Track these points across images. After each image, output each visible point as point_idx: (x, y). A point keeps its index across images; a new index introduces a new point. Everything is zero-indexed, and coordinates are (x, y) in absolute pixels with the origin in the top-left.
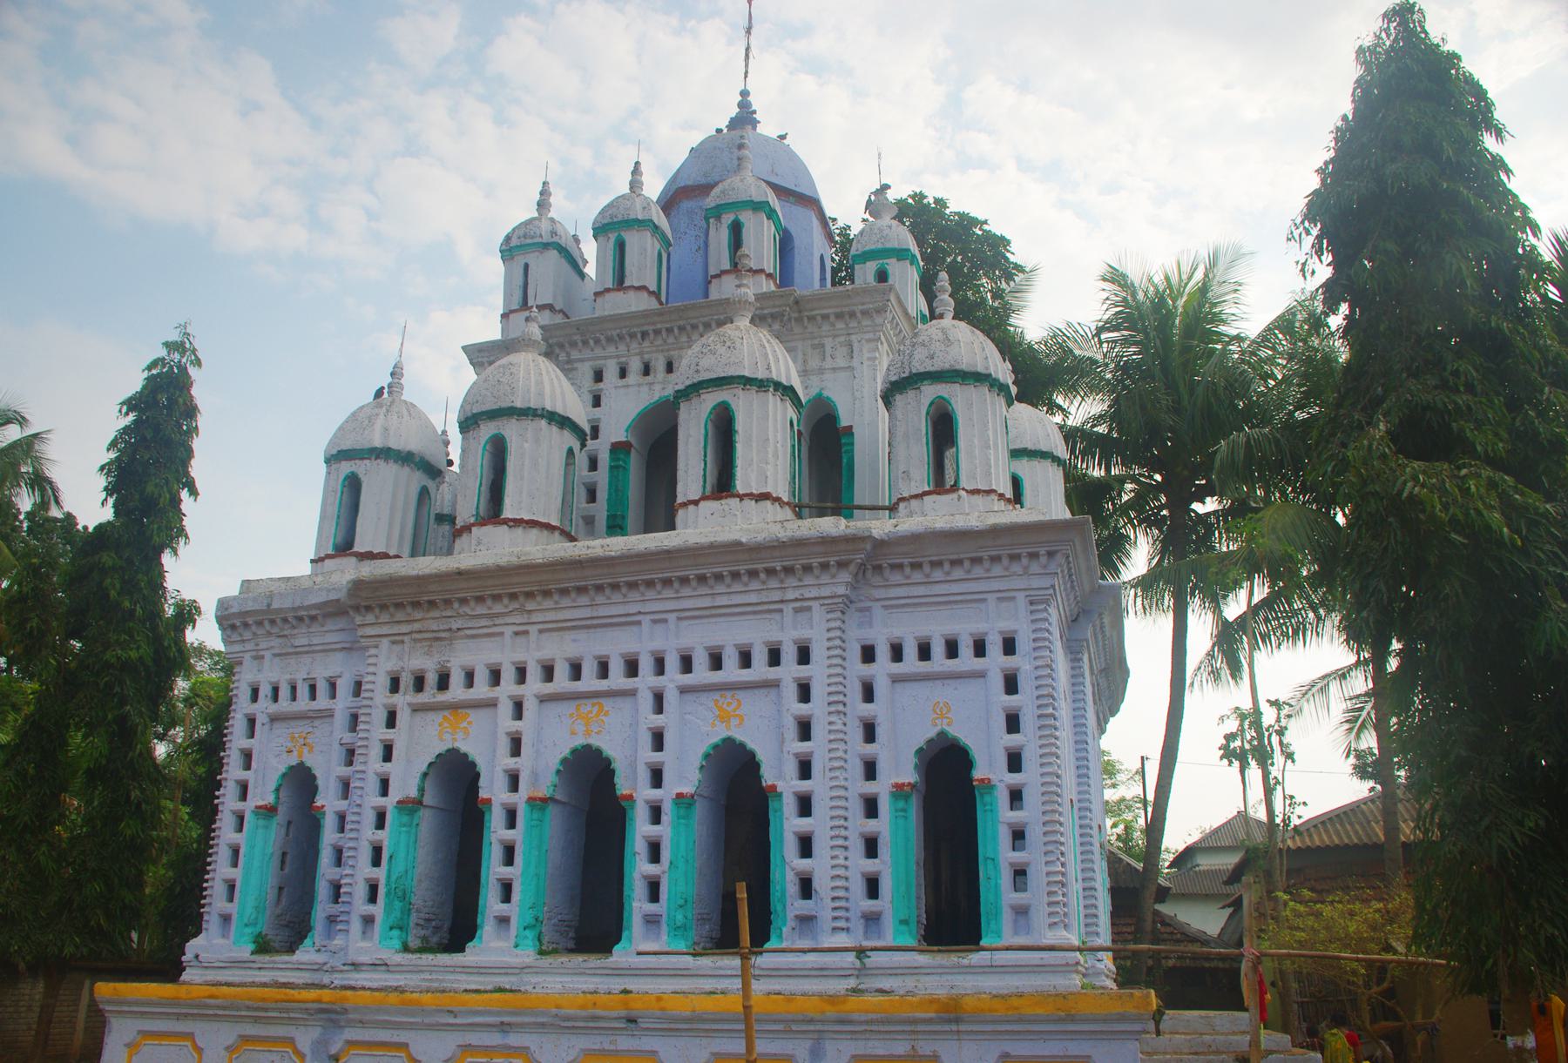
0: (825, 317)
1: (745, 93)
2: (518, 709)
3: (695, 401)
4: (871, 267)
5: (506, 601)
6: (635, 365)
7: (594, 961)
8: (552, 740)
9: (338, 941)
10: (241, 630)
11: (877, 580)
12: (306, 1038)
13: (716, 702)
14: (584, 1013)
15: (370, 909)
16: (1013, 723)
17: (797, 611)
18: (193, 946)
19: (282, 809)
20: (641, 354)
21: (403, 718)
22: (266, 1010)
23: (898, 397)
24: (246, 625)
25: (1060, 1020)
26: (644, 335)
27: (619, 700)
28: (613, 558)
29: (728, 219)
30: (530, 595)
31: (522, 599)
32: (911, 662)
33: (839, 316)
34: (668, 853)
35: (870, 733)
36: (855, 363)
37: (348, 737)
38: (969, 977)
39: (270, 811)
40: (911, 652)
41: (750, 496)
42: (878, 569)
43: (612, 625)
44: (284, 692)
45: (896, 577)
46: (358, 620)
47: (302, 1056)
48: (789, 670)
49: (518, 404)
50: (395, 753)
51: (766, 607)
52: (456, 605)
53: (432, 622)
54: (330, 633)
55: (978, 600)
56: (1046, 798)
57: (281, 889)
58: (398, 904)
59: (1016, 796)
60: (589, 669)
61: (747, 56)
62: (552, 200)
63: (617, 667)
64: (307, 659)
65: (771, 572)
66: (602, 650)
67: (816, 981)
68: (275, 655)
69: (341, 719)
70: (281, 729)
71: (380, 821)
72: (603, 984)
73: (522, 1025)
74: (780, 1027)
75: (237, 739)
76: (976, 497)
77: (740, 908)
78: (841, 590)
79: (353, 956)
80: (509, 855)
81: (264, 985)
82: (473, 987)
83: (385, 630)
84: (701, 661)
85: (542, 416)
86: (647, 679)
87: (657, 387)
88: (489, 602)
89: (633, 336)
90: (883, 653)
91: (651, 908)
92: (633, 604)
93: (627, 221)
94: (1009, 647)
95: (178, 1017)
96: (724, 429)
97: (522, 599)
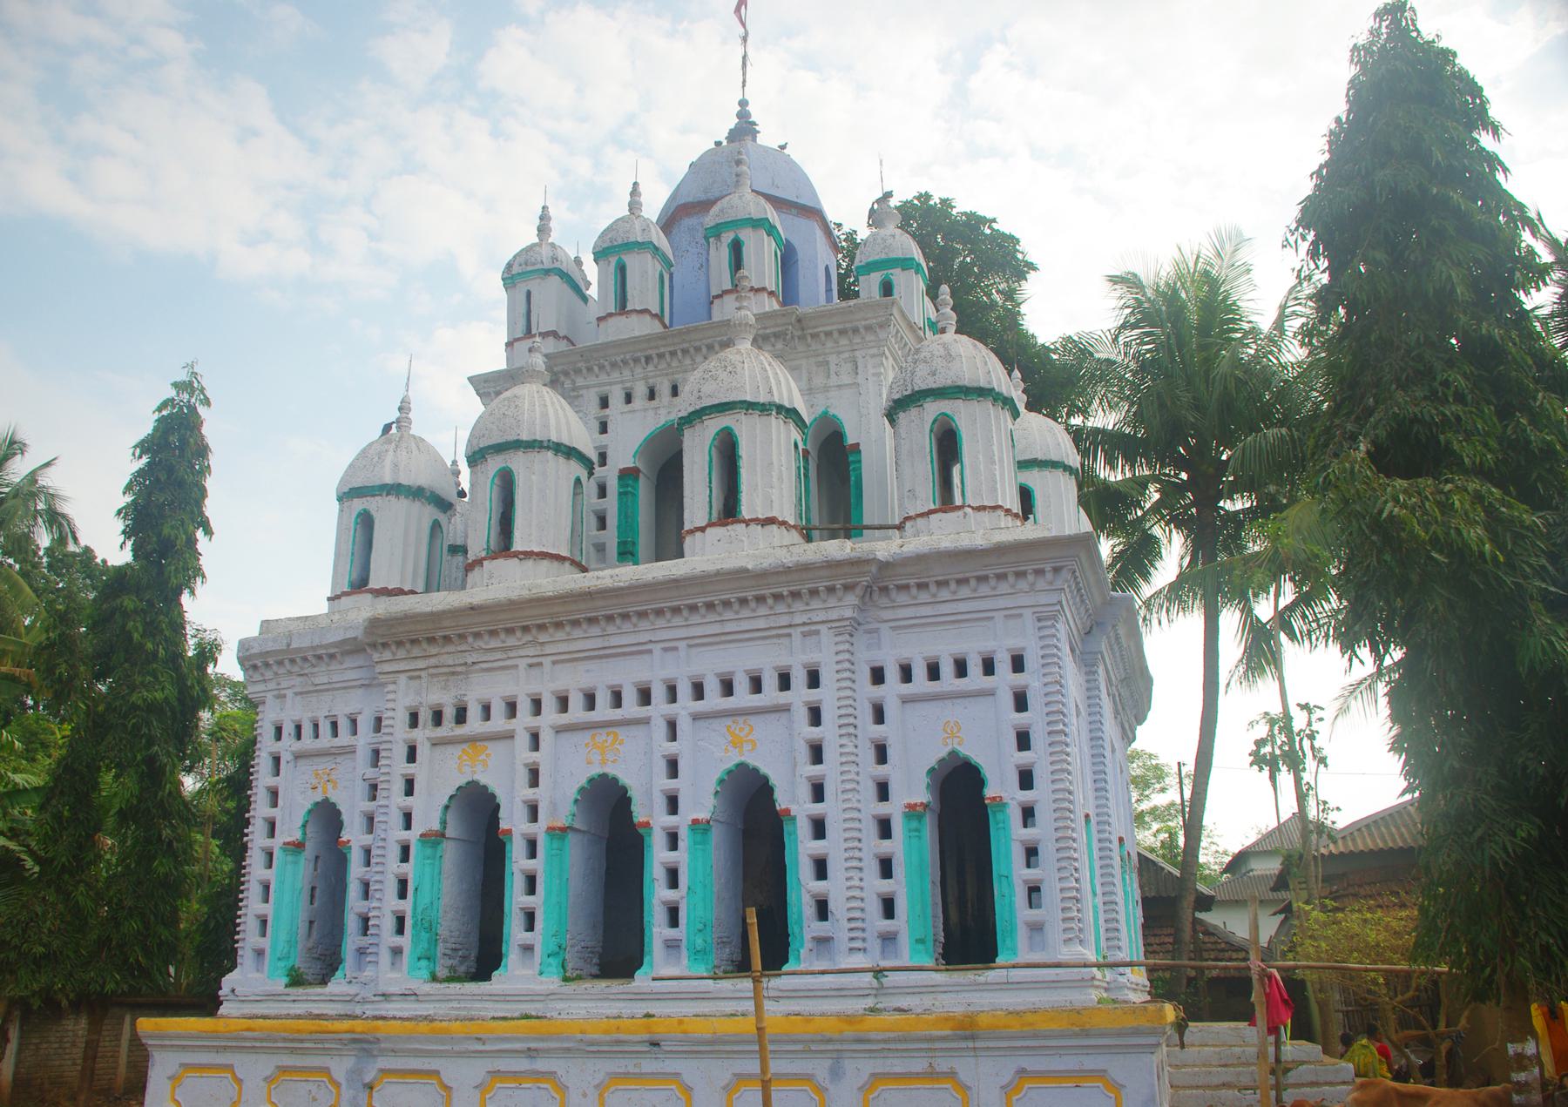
0: (828, 334)
1: (743, 103)
3: (698, 427)
4: (876, 278)
5: (519, 634)
6: (640, 390)
7: (616, 986)
8: (569, 769)
9: (369, 972)
10: (262, 670)
11: (884, 601)
12: (340, 1067)
14: (608, 1038)
15: (398, 940)
16: (1023, 741)
17: (805, 635)
18: (228, 981)
19: (308, 845)
20: (645, 378)
22: (302, 1041)
23: (901, 415)
24: (267, 665)
25: (1076, 1035)
26: (648, 359)
27: (633, 728)
28: (622, 589)
29: (728, 238)
30: (542, 627)
31: (534, 631)
33: (842, 332)
34: (687, 878)
35: (881, 754)
36: (860, 379)
37: (371, 773)
38: (985, 994)
39: (298, 846)
40: (920, 672)
41: (756, 520)
43: (624, 654)
44: (307, 730)
45: (902, 598)
46: (376, 656)
47: (337, 1085)
48: (800, 694)
49: (525, 437)
51: (774, 632)
52: (470, 639)
53: (448, 656)
54: (348, 671)
55: (985, 617)
57: (311, 922)
58: (425, 935)
59: (1028, 814)
60: (603, 699)
61: (744, 64)
63: (630, 696)
65: (778, 597)
66: (615, 680)
67: (834, 1001)
69: (363, 755)
71: (405, 855)
72: (626, 1008)
73: (548, 1051)
75: (262, 777)
76: (982, 513)
77: (762, 932)
78: (848, 613)
79: (382, 989)
80: (531, 884)
81: (299, 1017)
83: (402, 666)
84: (712, 687)
85: (548, 448)
86: (660, 707)
87: (663, 411)
88: (503, 636)
89: (636, 360)
90: (892, 674)
92: (643, 632)
94: (1018, 664)
95: (218, 1049)
96: (728, 452)
97: (534, 631)
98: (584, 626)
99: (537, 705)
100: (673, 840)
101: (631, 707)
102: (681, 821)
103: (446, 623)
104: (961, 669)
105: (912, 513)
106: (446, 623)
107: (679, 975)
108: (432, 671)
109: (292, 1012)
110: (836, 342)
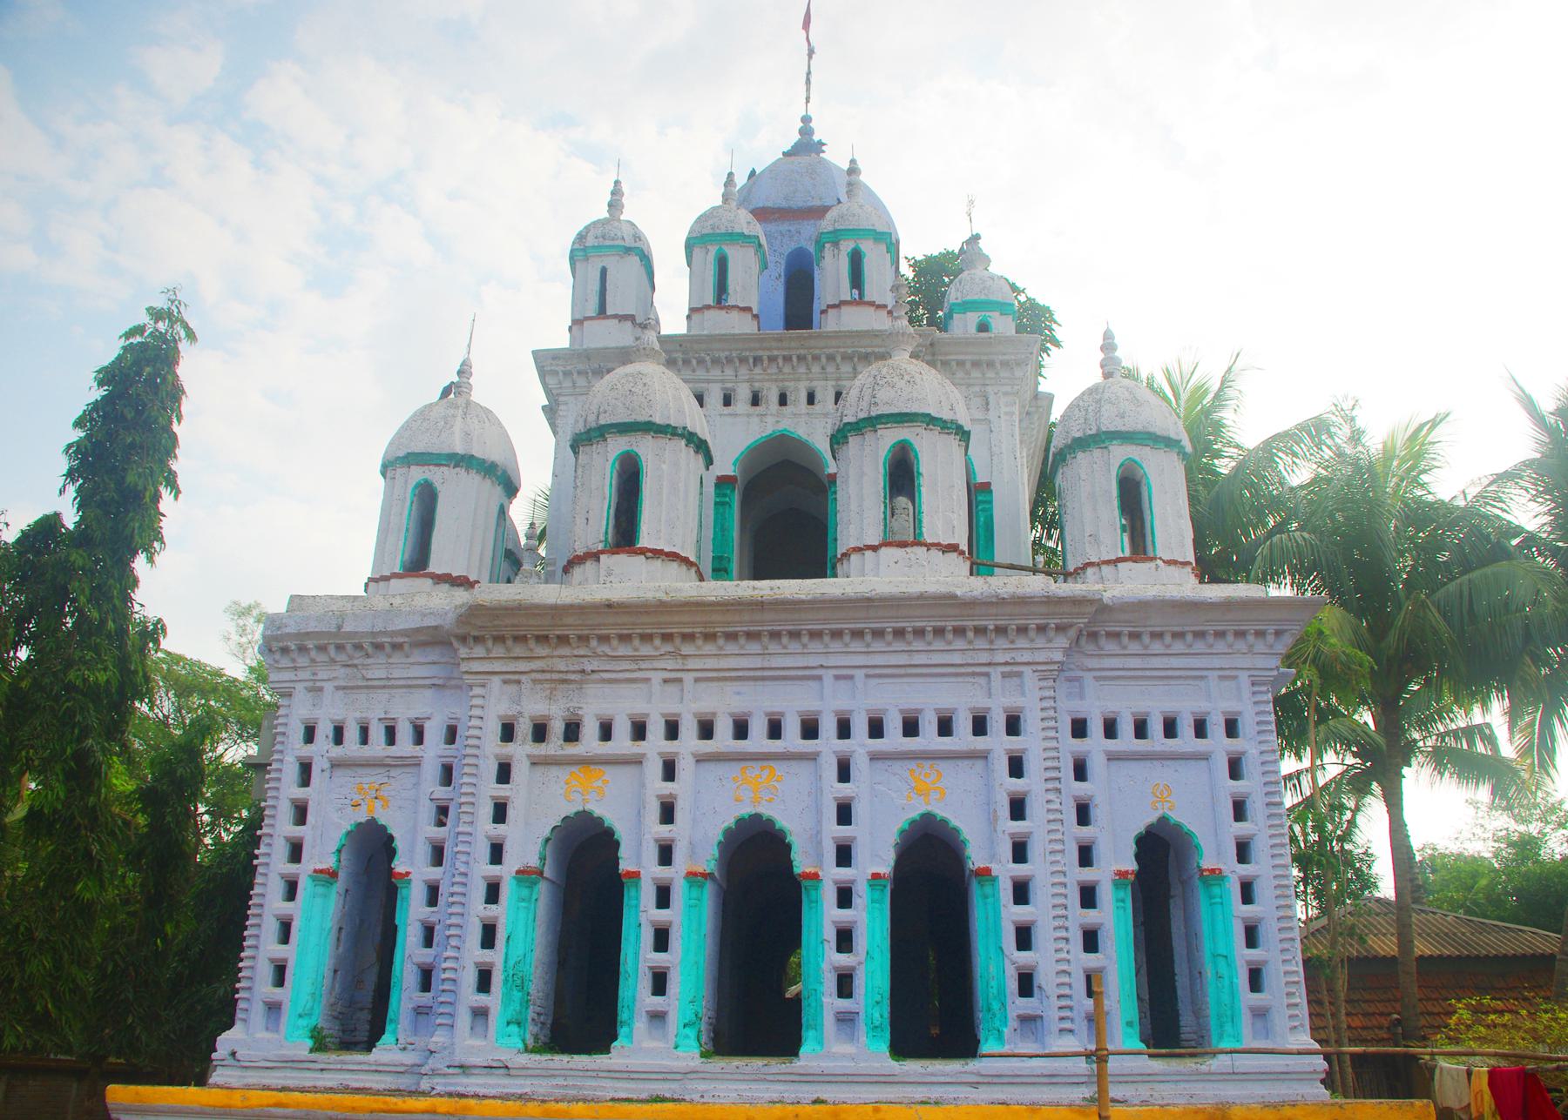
0: (961, 364)
1: (806, 120)
2: (669, 772)
3: (869, 436)
4: (973, 319)
5: (657, 642)
6: (743, 393)
7: (776, 1065)
8: (711, 809)
9: (439, 1038)
10: (295, 655)
11: (1089, 648)
15: (482, 999)
16: (1239, 811)
17: (1005, 675)
18: (227, 1041)
19: (342, 875)
21: (520, 771)
23: (1080, 455)
24: (302, 649)
26: (757, 360)
27: (793, 763)
28: (803, 602)
29: (847, 247)
30: (688, 637)
31: (678, 641)
32: (1126, 740)
33: (976, 364)
34: (848, 946)
35: (1083, 814)
36: (992, 415)
37: (442, 792)
38: (1208, 1085)
40: (1126, 728)
41: (937, 545)
42: (1093, 636)
44: (351, 734)
45: (1110, 646)
46: (463, 652)
48: (998, 742)
49: (658, 420)
50: (510, 813)
51: (970, 670)
52: (594, 643)
54: (418, 666)
56: (1278, 892)
58: (517, 995)
60: (758, 728)
61: (808, 81)
62: (624, 200)
63: (792, 728)
64: (383, 695)
65: (980, 631)
67: (1045, 1089)
68: (338, 688)
69: (431, 771)
70: (342, 776)
72: (790, 1092)
76: (1172, 568)
78: (1058, 656)
79: (460, 1058)
80: (662, 939)
81: (331, 1090)
82: (623, 1095)
84: (893, 726)
85: (682, 436)
86: (828, 744)
87: (770, 420)
88: (636, 642)
89: (743, 360)
90: (1096, 728)
91: (844, 1004)
94: (1231, 728)
97: (678, 641)
98: (742, 640)
99: (672, 730)
103: (570, 620)
104: (1170, 729)
105: (1094, 559)
106: (570, 620)
108: (534, 675)
109: (320, 1084)
110: (968, 373)
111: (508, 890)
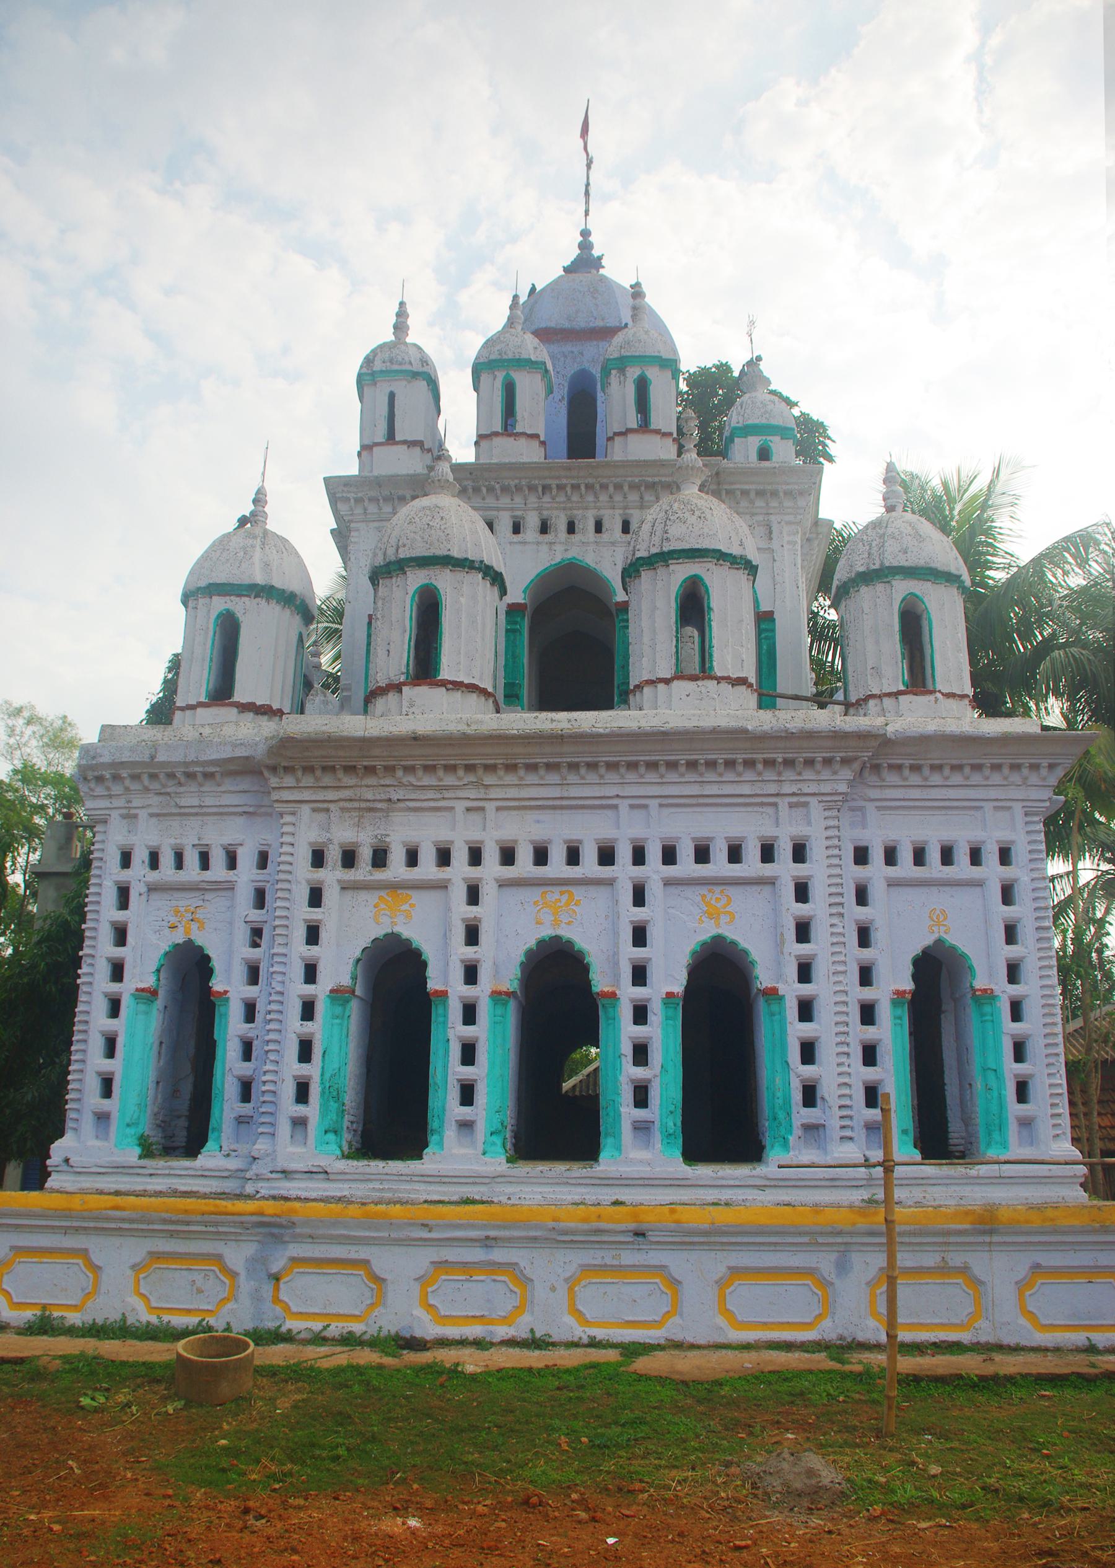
0: (745, 493)
1: (585, 233)
2: (473, 896)
3: (661, 571)
4: (754, 443)
5: (461, 773)
6: (532, 521)
8: (513, 933)
9: (261, 1146)
11: (872, 779)
12: (237, 1255)
13: (703, 896)
14: (586, 1227)
15: (301, 1110)
16: (1011, 934)
18: (59, 1149)
19: (161, 993)
20: (539, 509)
21: (331, 896)
22: (188, 1223)
23: (864, 589)
24: (116, 778)
25: (1095, 1231)
26: (546, 488)
28: (601, 735)
29: (633, 373)
30: (490, 768)
31: (480, 772)
32: (906, 867)
33: (760, 493)
34: (640, 1058)
35: (864, 937)
36: (775, 544)
37: (256, 915)
38: (977, 1188)
39: (150, 994)
40: (906, 855)
41: (727, 679)
42: (876, 768)
43: (583, 807)
44: (167, 859)
45: (892, 778)
46: (274, 781)
47: (233, 1275)
48: (785, 869)
49: (456, 553)
52: (400, 773)
53: (369, 790)
54: (230, 794)
55: (974, 807)
56: (1046, 1011)
57: (158, 1083)
58: (334, 1105)
60: (557, 855)
61: (587, 193)
62: (410, 322)
63: (589, 855)
64: (194, 822)
65: (769, 763)
66: (574, 834)
67: (827, 1191)
68: (151, 815)
69: (244, 895)
70: (160, 901)
71: (308, 1011)
72: (591, 1195)
73: (510, 1240)
74: (806, 1239)
75: (103, 912)
76: (951, 701)
77: (723, 1119)
78: (843, 788)
79: (281, 1164)
80: (469, 1054)
81: (158, 1194)
82: (436, 1198)
83: (306, 795)
84: (685, 853)
85: (479, 569)
86: (624, 870)
87: (559, 548)
88: (441, 773)
89: (532, 488)
90: (877, 855)
91: (641, 1114)
92: (609, 786)
93: (519, 361)
94: (1005, 856)
95: (66, 1231)
97: (480, 772)
98: (542, 772)
100: (470, 1014)
101: (428, 867)
102: (481, 992)
103: (376, 752)
104: (947, 856)
105: (876, 691)
106: (376, 752)
107: (642, 1156)
108: (342, 804)
109: (149, 1187)
110: (752, 502)
111: (321, 1009)
